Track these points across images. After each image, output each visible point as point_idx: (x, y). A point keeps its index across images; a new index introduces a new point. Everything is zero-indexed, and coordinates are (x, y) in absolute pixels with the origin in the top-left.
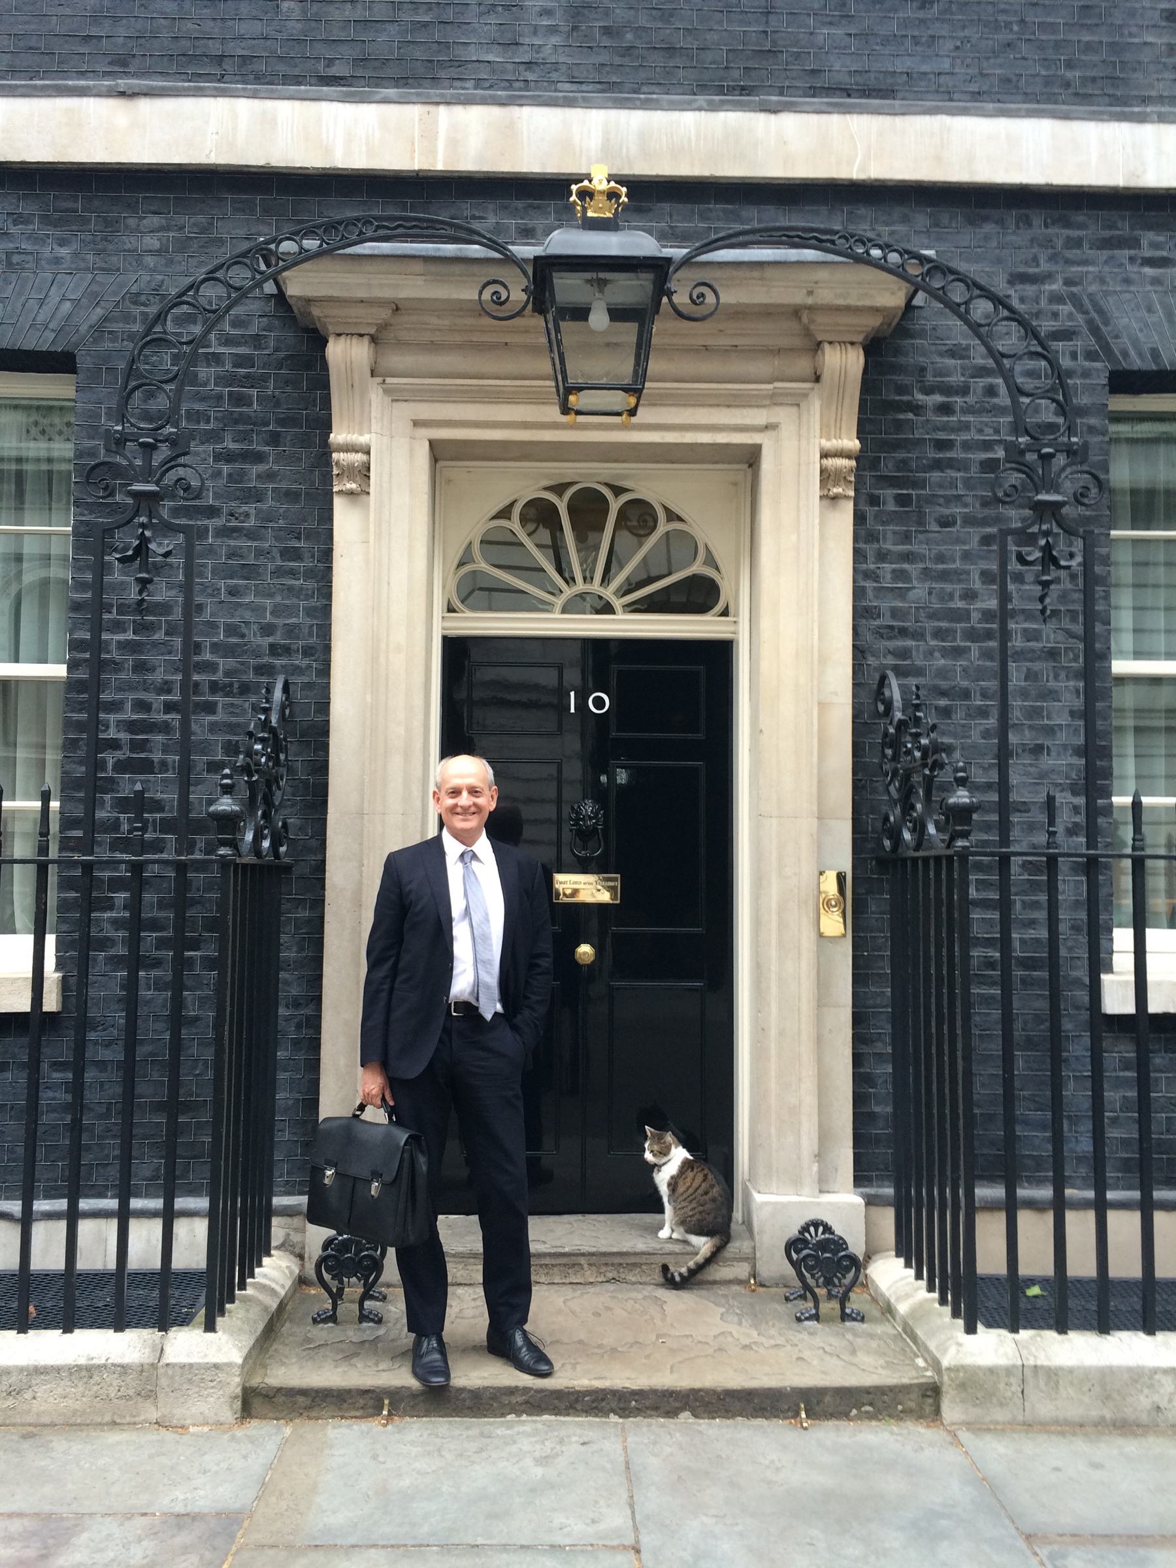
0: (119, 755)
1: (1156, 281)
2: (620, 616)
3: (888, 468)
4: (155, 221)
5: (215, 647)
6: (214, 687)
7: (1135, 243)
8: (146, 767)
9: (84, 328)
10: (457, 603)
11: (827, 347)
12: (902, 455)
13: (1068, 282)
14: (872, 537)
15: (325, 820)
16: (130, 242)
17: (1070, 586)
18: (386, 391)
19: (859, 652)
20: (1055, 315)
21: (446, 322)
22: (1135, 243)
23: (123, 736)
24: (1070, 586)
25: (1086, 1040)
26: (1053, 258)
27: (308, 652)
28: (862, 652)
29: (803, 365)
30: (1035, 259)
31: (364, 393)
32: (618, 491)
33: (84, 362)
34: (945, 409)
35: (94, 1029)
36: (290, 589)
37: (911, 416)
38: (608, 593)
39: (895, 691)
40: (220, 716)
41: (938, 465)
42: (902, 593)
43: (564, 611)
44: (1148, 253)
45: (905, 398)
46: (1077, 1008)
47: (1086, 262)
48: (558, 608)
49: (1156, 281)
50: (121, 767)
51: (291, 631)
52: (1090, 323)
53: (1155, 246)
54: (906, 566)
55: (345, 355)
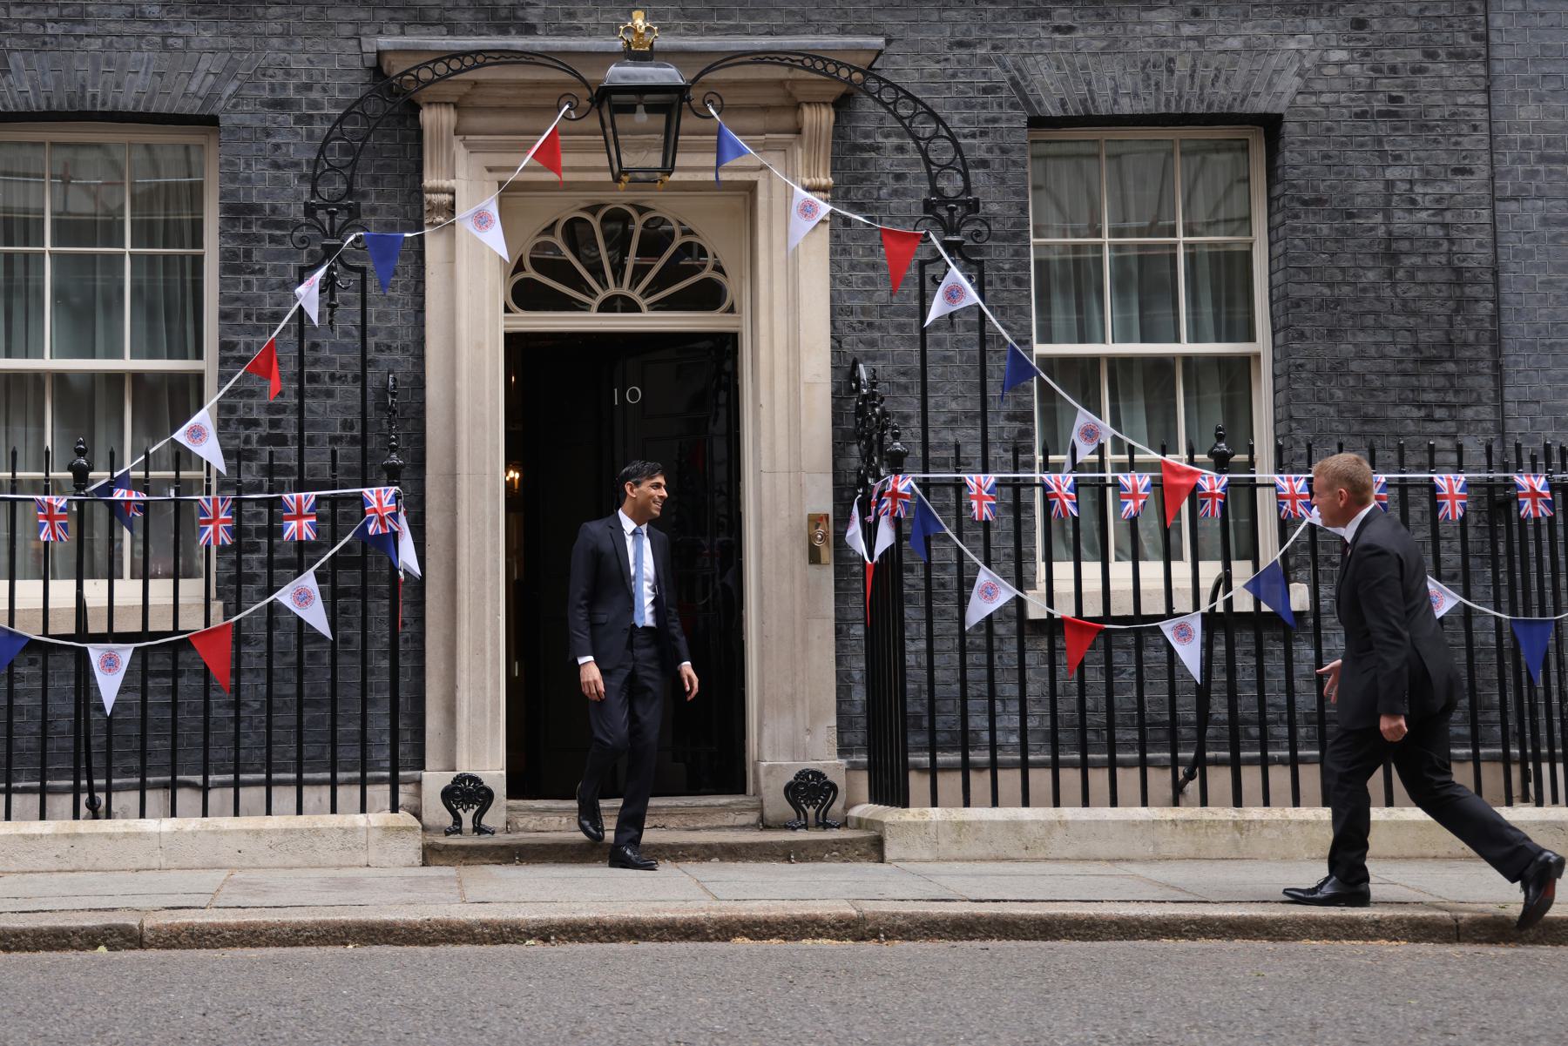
0: (264, 430)
1: (1063, 45)
2: (646, 314)
3: (857, 196)
4: (276, 10)
5: (333, 346)
6: (333, 377)
7: (1047, 14)
8: (281, 441)
9: (225, 97)
10: (512, 305)
11: (806, 109)
12: (866, 185)
13: (995, 48)
14: (845, 251)
15: (423, 480)
16: (260, 27)
17: (999, 287)
18: (466, 146)
19: (837, 339)
20: (985, 73)
21: (511, 92)
22: (1047, 14)
23: (264, 417)
24: (999, 287)
25: (1015, 642)
26: (983, 28)
27: (404, 349)
28: (839, 342)
29: (787, 120)
30: (969, 30)
31: (449, 147)
32: (642, 210)
33: (223, 123)
34: (900, 149)
35: (249, 644)
36: (390, 299)
37: (873, 154)
38: (635, 295)
39: (864, 375)
40: (337, 401)
41: (895, 193)
42: (870, 294)
43: (599, 310)
44: (1058, 22)
45: (868, 141)
46: (1008, 617)
47: (1009, 31)
48: (595, 308)
49: (1063, 45)
50: (264, 440)
51: (392, 333)
52: (1012, 79)
53: (1063, 17)
54: (872, 274)
55: (435, 119)
